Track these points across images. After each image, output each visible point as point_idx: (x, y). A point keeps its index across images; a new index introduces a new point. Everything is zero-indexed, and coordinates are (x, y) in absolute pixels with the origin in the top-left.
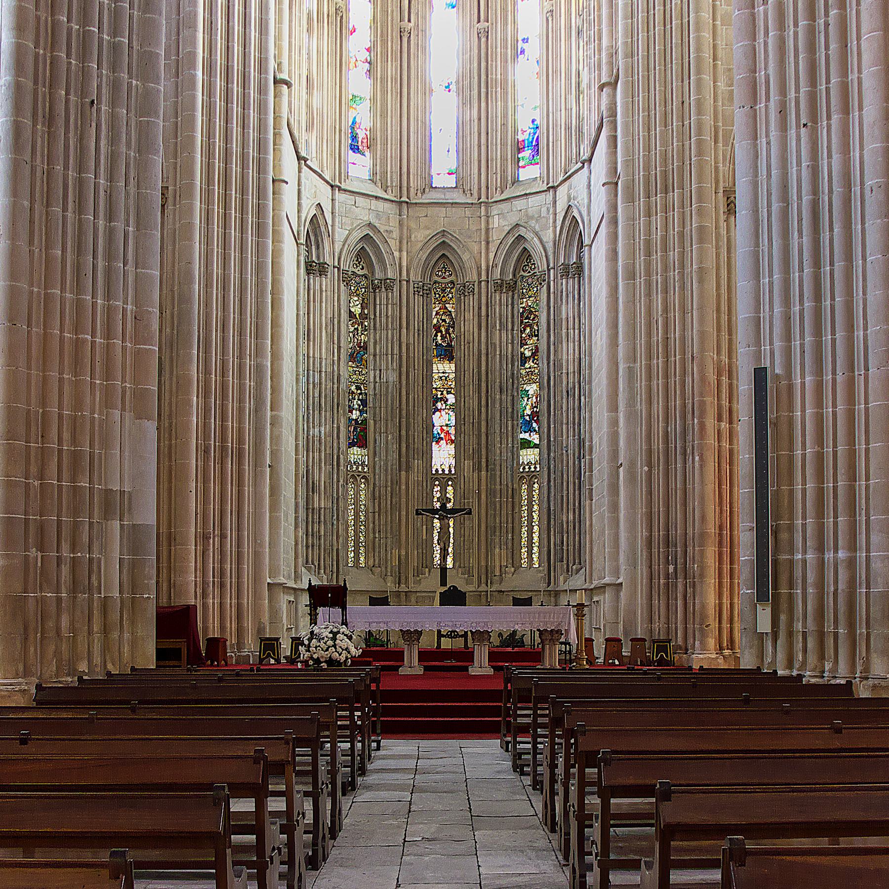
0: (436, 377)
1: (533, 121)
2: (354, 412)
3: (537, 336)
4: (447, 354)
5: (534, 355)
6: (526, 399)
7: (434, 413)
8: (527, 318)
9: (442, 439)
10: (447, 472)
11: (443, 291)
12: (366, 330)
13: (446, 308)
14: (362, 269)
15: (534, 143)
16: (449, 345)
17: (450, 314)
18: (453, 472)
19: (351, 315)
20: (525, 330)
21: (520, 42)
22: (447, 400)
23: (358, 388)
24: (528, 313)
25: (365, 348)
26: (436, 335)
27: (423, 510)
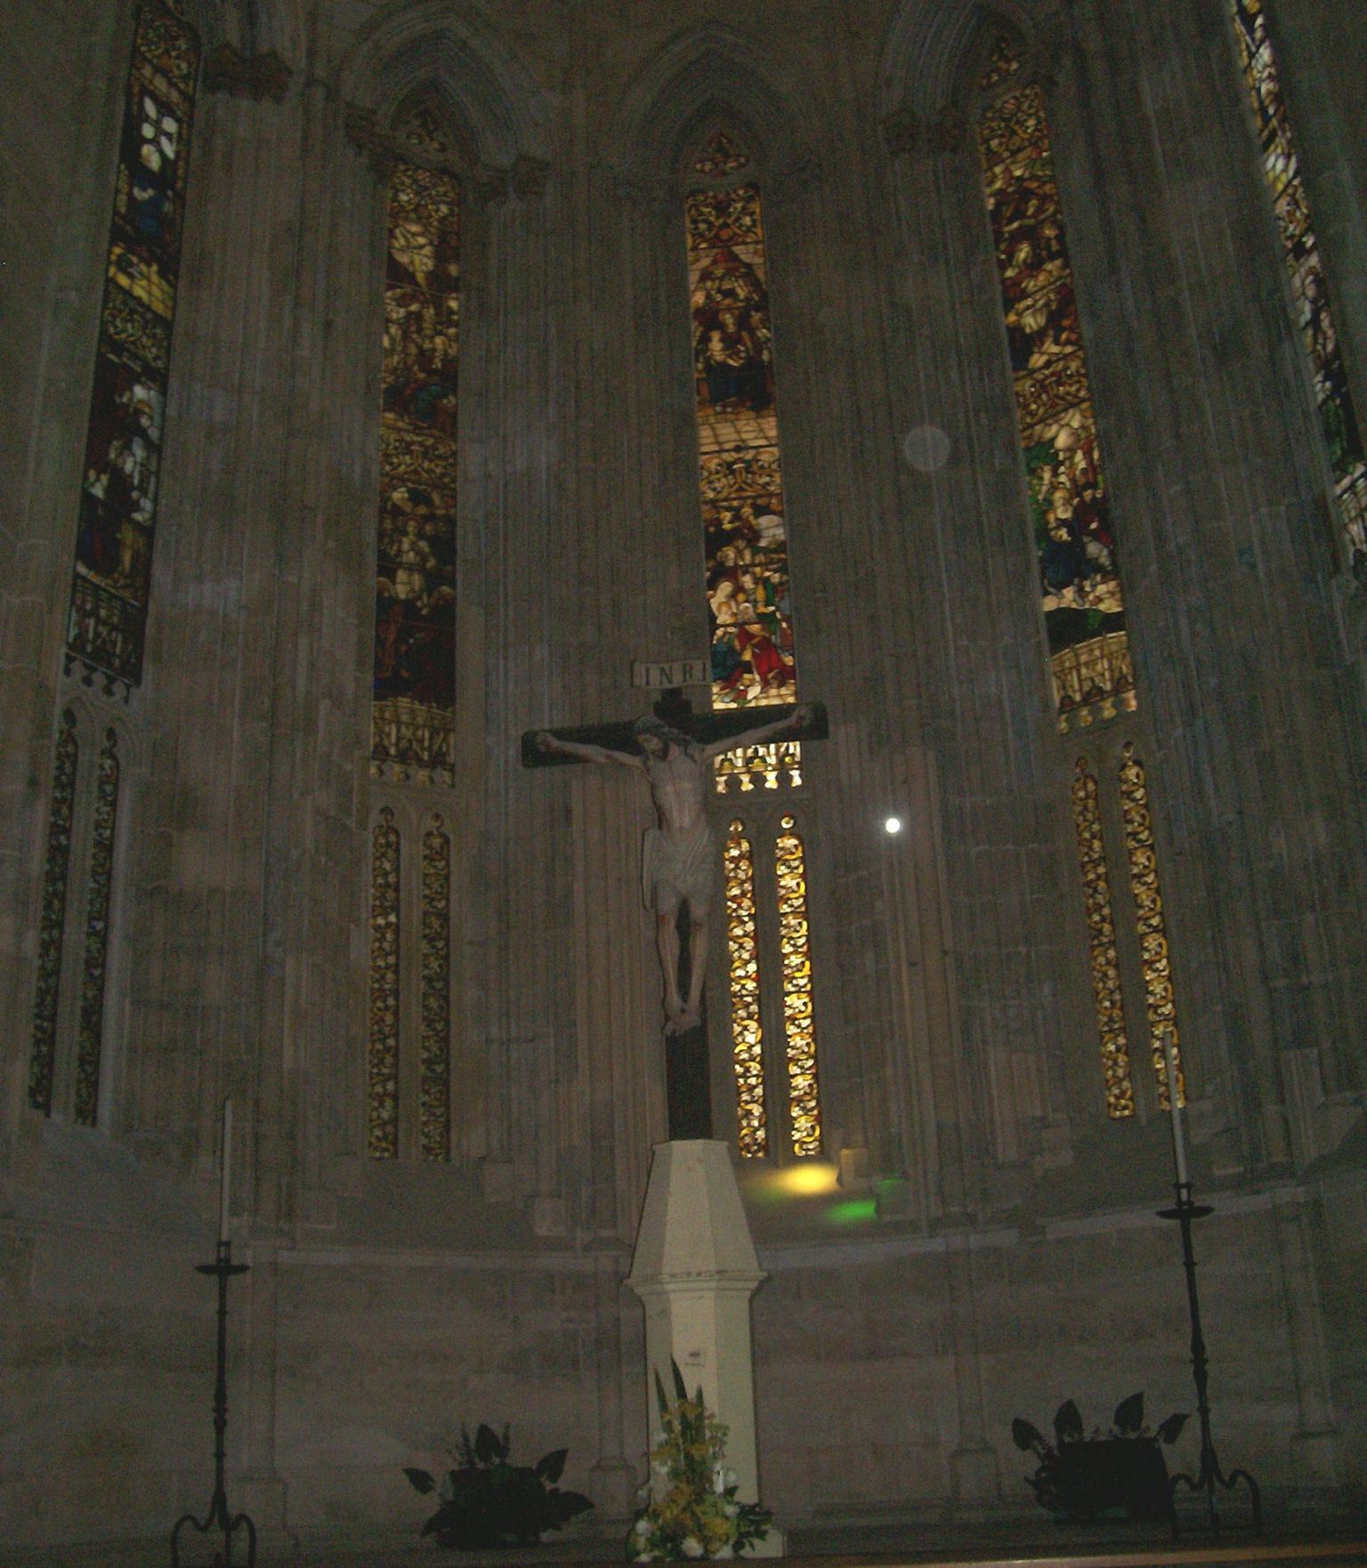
2: (401, 575)
3: (1063, 253)
4: (746, 388)
5: (1055, 320)
6: (1047, 476)
7: (713, 585)
8: (1019, 214)
9: (747, 668)
10: (771, 782)
11: (722, 208)
13: (736, 258)
14: (443, 148)
16: (753, 363)
17: (749, 273)
18: (797, 781)
19: (398, 274)
20: (1011, 254)
23: (417, 497)
24: (1017, 196)
25: (449, 376)
26: (705, 339)
27: (560, 734)
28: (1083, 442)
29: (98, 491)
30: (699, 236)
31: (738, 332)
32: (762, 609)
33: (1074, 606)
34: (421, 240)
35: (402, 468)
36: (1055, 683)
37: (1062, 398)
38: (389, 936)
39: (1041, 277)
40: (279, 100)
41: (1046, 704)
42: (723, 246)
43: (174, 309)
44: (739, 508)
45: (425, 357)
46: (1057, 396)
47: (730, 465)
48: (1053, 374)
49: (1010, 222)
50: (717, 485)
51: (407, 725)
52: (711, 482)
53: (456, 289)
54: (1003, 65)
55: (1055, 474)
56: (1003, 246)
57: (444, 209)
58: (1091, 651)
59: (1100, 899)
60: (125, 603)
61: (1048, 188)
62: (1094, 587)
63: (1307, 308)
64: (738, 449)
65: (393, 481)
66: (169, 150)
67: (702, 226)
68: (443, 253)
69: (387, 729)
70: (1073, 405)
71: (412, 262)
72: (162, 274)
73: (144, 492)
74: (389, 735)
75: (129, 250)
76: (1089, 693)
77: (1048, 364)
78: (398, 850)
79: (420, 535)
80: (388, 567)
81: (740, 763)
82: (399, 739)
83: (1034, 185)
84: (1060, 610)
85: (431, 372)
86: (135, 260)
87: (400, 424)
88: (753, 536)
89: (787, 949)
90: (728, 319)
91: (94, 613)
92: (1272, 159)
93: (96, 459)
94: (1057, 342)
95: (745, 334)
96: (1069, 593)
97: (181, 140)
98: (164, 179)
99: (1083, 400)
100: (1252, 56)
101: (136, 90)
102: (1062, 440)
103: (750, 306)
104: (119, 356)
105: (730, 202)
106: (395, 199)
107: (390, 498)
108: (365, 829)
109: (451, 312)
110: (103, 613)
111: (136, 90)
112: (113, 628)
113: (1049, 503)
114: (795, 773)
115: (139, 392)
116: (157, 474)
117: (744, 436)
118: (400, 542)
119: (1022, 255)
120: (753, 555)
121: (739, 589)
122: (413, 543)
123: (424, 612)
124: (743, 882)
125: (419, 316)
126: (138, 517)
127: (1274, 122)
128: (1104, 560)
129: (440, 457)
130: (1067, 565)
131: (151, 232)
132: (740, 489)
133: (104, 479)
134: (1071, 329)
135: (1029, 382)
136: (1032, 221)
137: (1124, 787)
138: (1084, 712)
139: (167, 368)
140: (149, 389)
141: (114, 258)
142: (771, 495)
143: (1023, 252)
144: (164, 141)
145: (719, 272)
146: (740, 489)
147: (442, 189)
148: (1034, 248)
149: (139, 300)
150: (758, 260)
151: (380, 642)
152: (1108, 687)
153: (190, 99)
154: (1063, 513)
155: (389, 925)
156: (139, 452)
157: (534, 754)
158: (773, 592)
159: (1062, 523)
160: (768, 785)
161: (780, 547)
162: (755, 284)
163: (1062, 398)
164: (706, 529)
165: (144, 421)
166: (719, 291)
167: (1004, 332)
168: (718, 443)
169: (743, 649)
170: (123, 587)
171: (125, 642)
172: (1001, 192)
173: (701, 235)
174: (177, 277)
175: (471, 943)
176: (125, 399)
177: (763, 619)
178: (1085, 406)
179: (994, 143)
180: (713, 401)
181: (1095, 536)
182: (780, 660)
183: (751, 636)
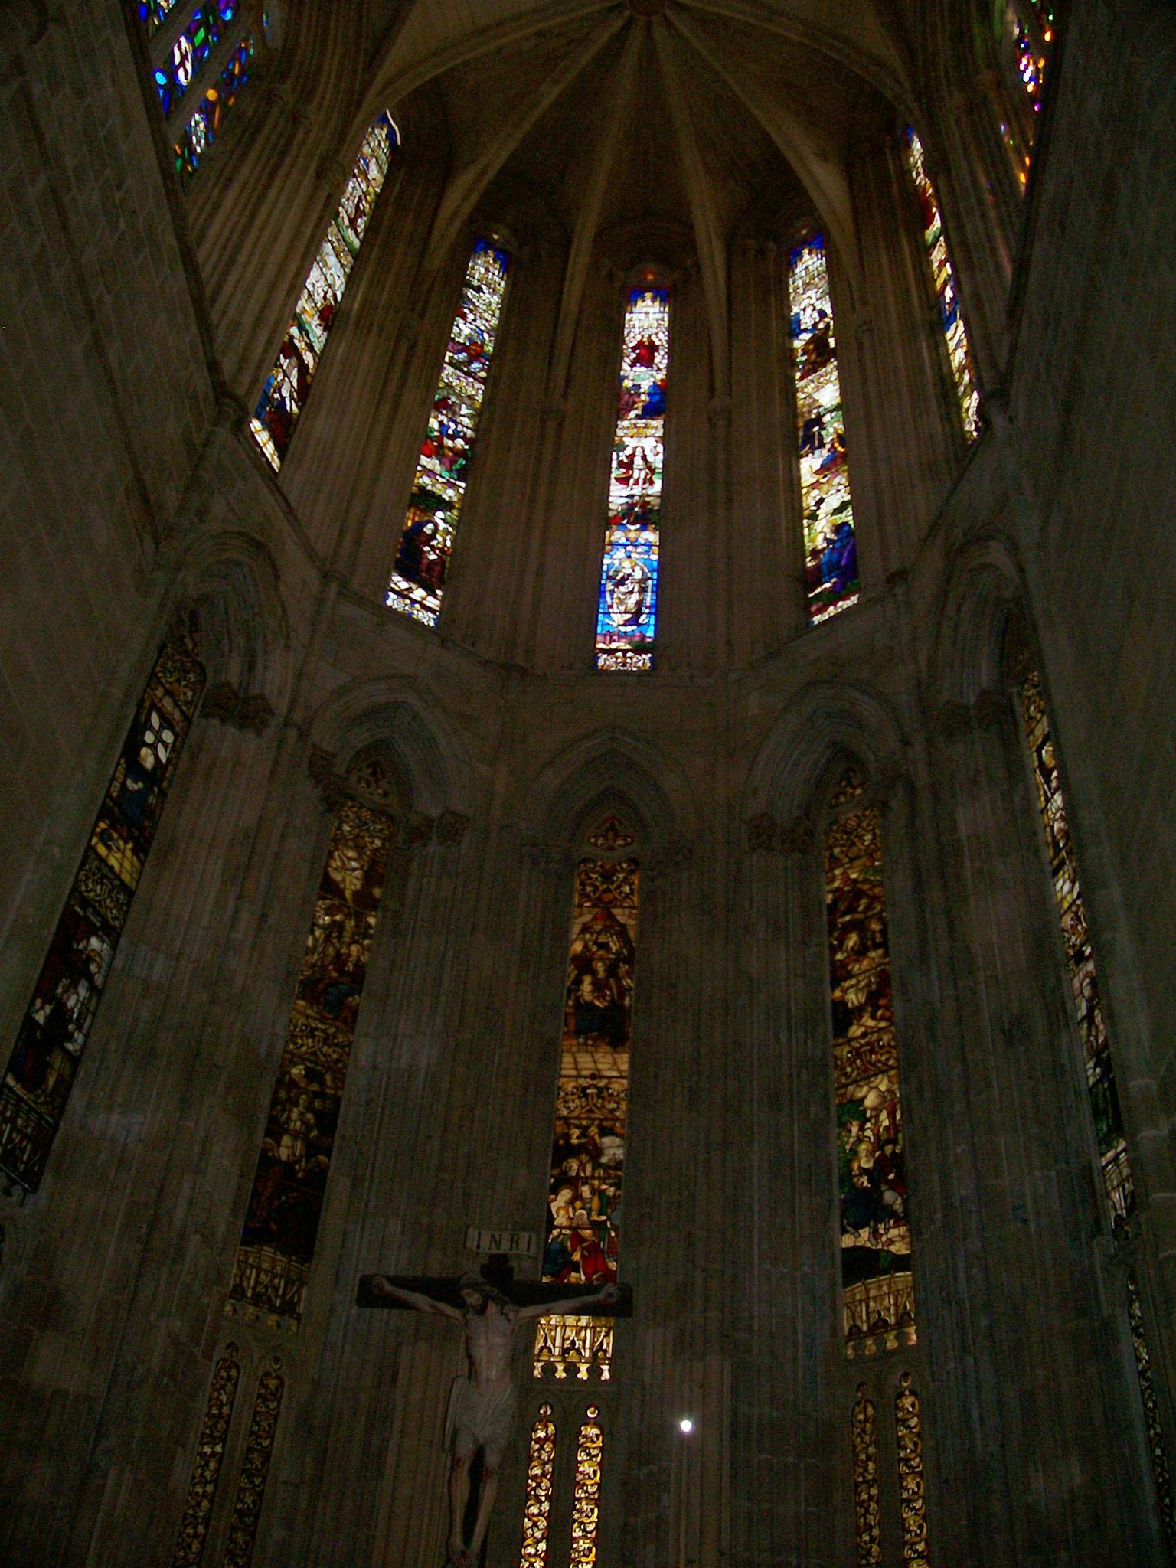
0: (570, 1086)
1: (838, 529)
2: (286, 1140)
3: (884, 945)
4: (606, 1027)
5: (874, 999)
6: (855, 1129)
7: (555, 1190)
8: (851, 909)
10: (583, 1375)
11: (607, 877)
12: (366, 936)
13: (612, 917)
14: (386, 794)
15: (843, 562)
16: (616, 1006)
17: (622, 932)
18: (606, 1375)
19: (330, 888)
20: (842, 941)
21: (801, 434)
22: (598, 1152)
23: (311, 1075)
24: (852, 894)
26: (578, 981)
27: (395, 1281)
28: (888, 1103)
29: (40, 1018)
30: (584, 895)
31: (607, 978)
32: (595, 1218)
33: (868, 1245)
34: (354, 864)
35: (304, 1049)
36: (846, 1313)
37: (873, 1065)
38: (212, 1465)
39: (865, 963)
40: (259, 733)
41: (835, 1330)
42: (605, 908)
43: (138, 882)
44: (588, 1127)
45: (340, 960)
46: (870, 1062)
47: (584, 1089)
48: (867, 1044)
49: (844, 914)
50: (571, 1105)
51: (266, 1272)
52: (566, 1102)
53: (374, 908)
54: (849, 790)
55: (862, 1129)
56: (836, 934)
57: (378, 843)
58: (880, 1287)
59: (871, 1519)
60: (41, 1117)
61: (877, 890)
62: (887, 1230)
63: (1084, 1005)
64: (593, 1077)
65: (294, 1059)
66: (163, 756)
67: (589, 889)
68: (371, 877)
69: (248, 1272)
70: (882, 1072)
71: (344, 880)
72: (134, 851)
73: (79, 1028)
74: (249, 1278)
75: (112, 826)
76: (875, 1323)
77: (864, 1035)
78: (235, 1385)
79: (309, 1108)
80: (276, 1130)
81: (557, 1352)
82: (257, 1282)
83: (866, 887)
84: (855, 1248)
85: (340, 970)
86: (115, 836)
87: (309, 1012)
88: (596, 1152)
89: (577, 1533)
90: (600, 967)
91: (12, 1121)
92: (1061, 882)
93: (44, 990)
94: (873, 1017)
95: (612, 981)
96: (865, 1233)
97: (174, 750)
98: (154, 777)
99: (892, 1068)
100: (1048, 800)
101: (147, 704)
102: (868, 1103)
103: (619, 958)
104: (84, 909)
105: (614, 872)
106: (339, 828)
107: (289, 1073)
108: (211, 1360)
109: (369, 926)
110: (20, 1122)
111: (147, 704)
112: (25, 1137)
113: (855, 1152)
114: (605, 1368)
115: (94, 942)
116: (94, 1015)
117: (600, 1066)
118: (291, 1111)
119: (851, 943)
120: (594, 1169)
121: (577, 1196)
122: (301, 1114)
123: (300, 1175)
124: (545, 1463)
125: (340, 927)
126: (69, 1046)
127: (1064, 853)
128: (898, 1207)
129: (336, 1045)
130: (865, 1208)
131: (134, 815)
132: (591, 1111)
133: (48, 1008)
134: (887, 1008)
135: (846, 1049)
136: (860, 916)
137: (900, 1415)
138: (869, 1342)
139: (122, 927)
140: (103, 942)
141: (98, 830)
142: (617, 1119)
143: (853, 940)
144: (160, 747)
145: (598, 928)
146: (591, 1111)
147: (379, 827)
148: (861, 938)
149: (111, 868)
150: (631, 922)
151: (256, 1194)
152: (892, 1320)
153: (188, 720)
154: (866, 1163)
155: (214, 1454)
156: (83, 992)
157: (369, 1295)
158: (607, 1204)
159: (864, 1171)
160: (579, 1376)
161: (618, 1165)
162: (627, 942)
163: (873, 1065)
164: (556, 1142)
165: (93, 968)
166: (595, 943)
167: (829, 1004)
168: (576, 1069)
169: (574, 1250)
170: (42, 1104)
171: (33, 1152)
172: (838, 889)
173: (588, 896)
174: (146, 856)
175: (284, 1483)
176: (81, 946)
177: (595, 1226)
178: (892, 1073)
179: (837, 850)
180: (577, 1033)
181: (893, 1185)
182: (605, 1264)
183: (585, 1240)
